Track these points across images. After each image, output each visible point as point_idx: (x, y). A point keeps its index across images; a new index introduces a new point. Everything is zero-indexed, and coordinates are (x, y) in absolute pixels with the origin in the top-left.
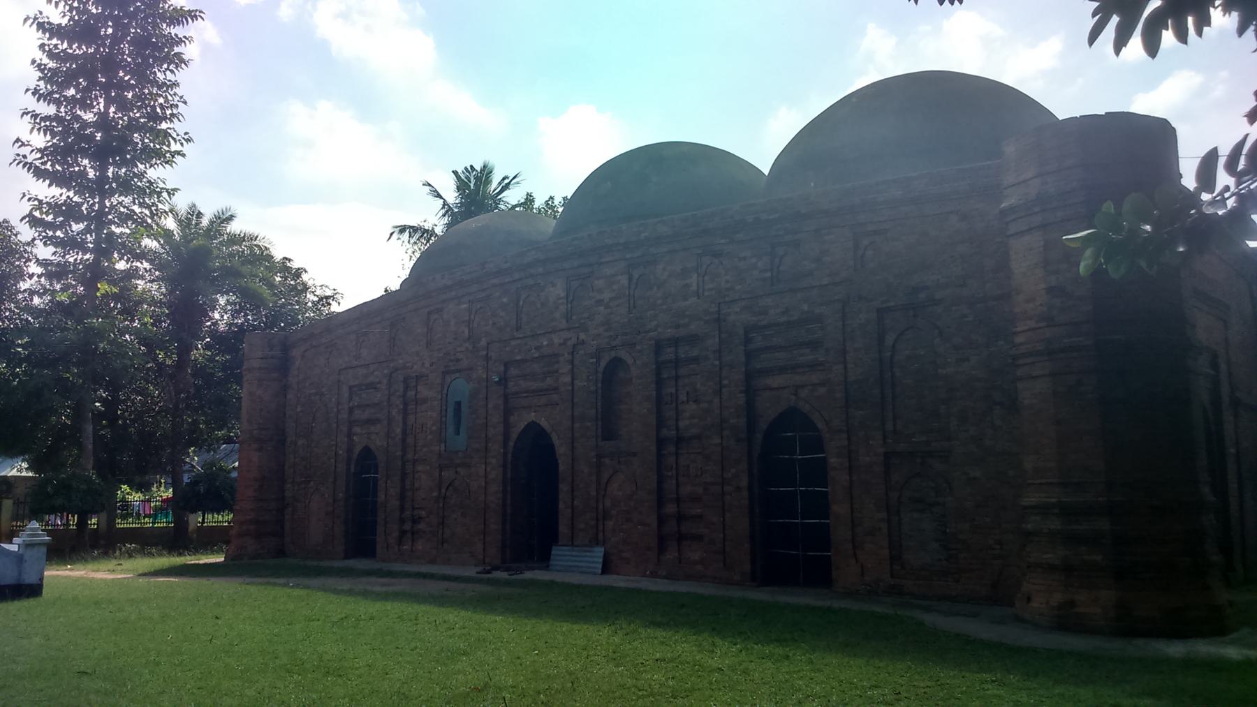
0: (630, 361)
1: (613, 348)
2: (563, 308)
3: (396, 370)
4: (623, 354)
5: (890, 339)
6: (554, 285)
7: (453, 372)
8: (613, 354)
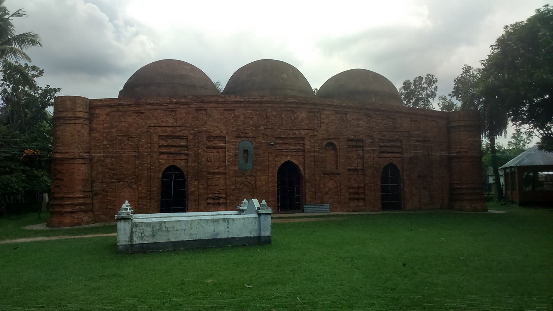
0: (336, 143)
1: (329, 139)
4: (333, 141)
6: (301, 113)
7: (242, 137)
8: (329, 141)
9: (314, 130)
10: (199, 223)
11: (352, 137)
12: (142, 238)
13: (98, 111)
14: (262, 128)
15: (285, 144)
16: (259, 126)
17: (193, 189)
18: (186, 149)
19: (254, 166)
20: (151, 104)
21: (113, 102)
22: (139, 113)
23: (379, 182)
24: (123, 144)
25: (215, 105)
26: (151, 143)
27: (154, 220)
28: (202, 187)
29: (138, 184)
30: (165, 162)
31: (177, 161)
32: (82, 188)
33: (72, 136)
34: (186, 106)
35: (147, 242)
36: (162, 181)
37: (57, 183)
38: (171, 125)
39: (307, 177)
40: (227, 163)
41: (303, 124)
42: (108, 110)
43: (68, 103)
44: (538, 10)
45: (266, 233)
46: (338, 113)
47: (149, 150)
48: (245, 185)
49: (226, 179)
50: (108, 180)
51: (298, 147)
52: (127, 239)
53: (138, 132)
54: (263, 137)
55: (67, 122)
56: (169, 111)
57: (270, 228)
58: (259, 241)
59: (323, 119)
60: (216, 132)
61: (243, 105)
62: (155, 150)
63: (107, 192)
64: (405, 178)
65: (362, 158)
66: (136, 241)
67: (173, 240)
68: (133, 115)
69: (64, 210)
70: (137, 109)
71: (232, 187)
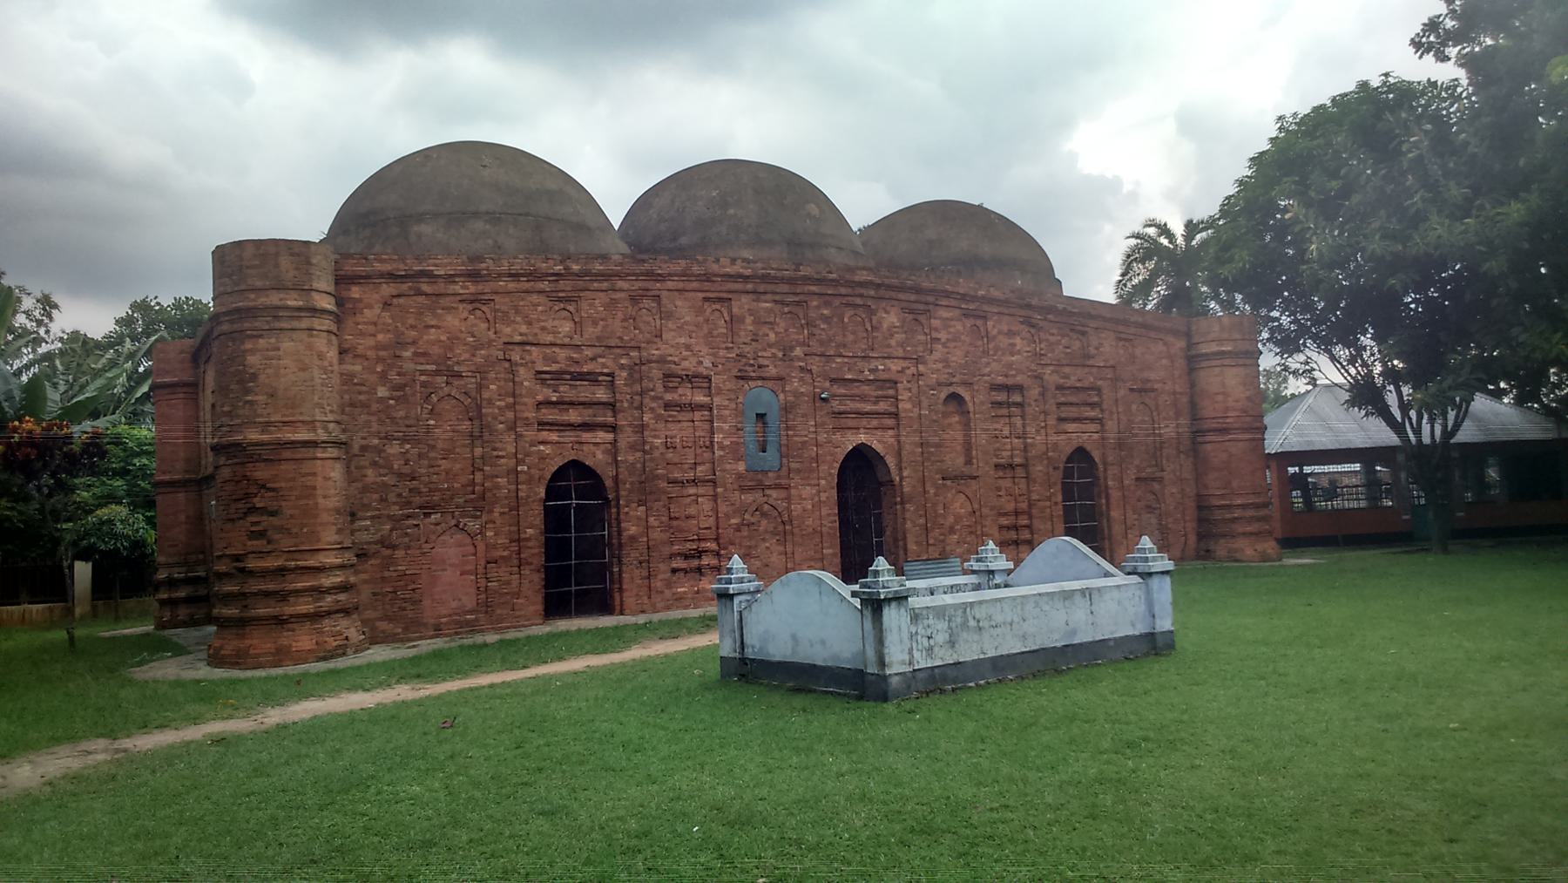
0: (967, 398)
1: (951, 384)
2: (899, 337)
3: (650, 362)
4: (961, 391)
5: (1134, 407)
6: (887, 312)
7: (752, 379)
8: (952, 389)
9: (918, 361)
10: (1037, 603)
11: (1000, 380)
12: (930, 649)
13: (355, 292)
14: (798, 351)
15: (852, 397)
16: (792, 348)
17: (633, 530)
18: (610, 413)
20: (510, 275)
21: (402, 266)
22: (475, 301)
23: (1060, 498)
24: (434, 398)
25: (681, 285)
26: (514, 395)
27: (949, 599)
28: (656, 524)
29: (484, 518)
30: (552, 451)
31: (585, 448)
32: (336, 538)
33: (303, 370)
34: (605, 285)
35: (939, 663)
36: (548, 511)
37: (253, 524)
38: (567, 341)
39: (906, 490)
40: (718, 453)
41: (893, 342)
42: (387, 289)
43: (285, 262)
44: (1364, 86)
45: (1165, 624)
46: (966, 314)
47: (510, 415)
48: (764, 515)
49: (715, 497)
50: (396, 511)
51: (882, 406)
52: (907, 657)
53: (479, 360)
54: (801, 379)
55: (284, 325)
56: (560, 300)
57: (1169, 608)
58: (1153, 645)
59: (936, 330)
60: (685, 364)
61: (750, 287)
62: (526, 414)
63: (394, 547)
64: (1110, 483)
65: (1023, 436)
66: (922, 662)
67: (991, 653)
68: (461, 306)
69: (289, 610)
70: (472, 288)
71: (733, 521)
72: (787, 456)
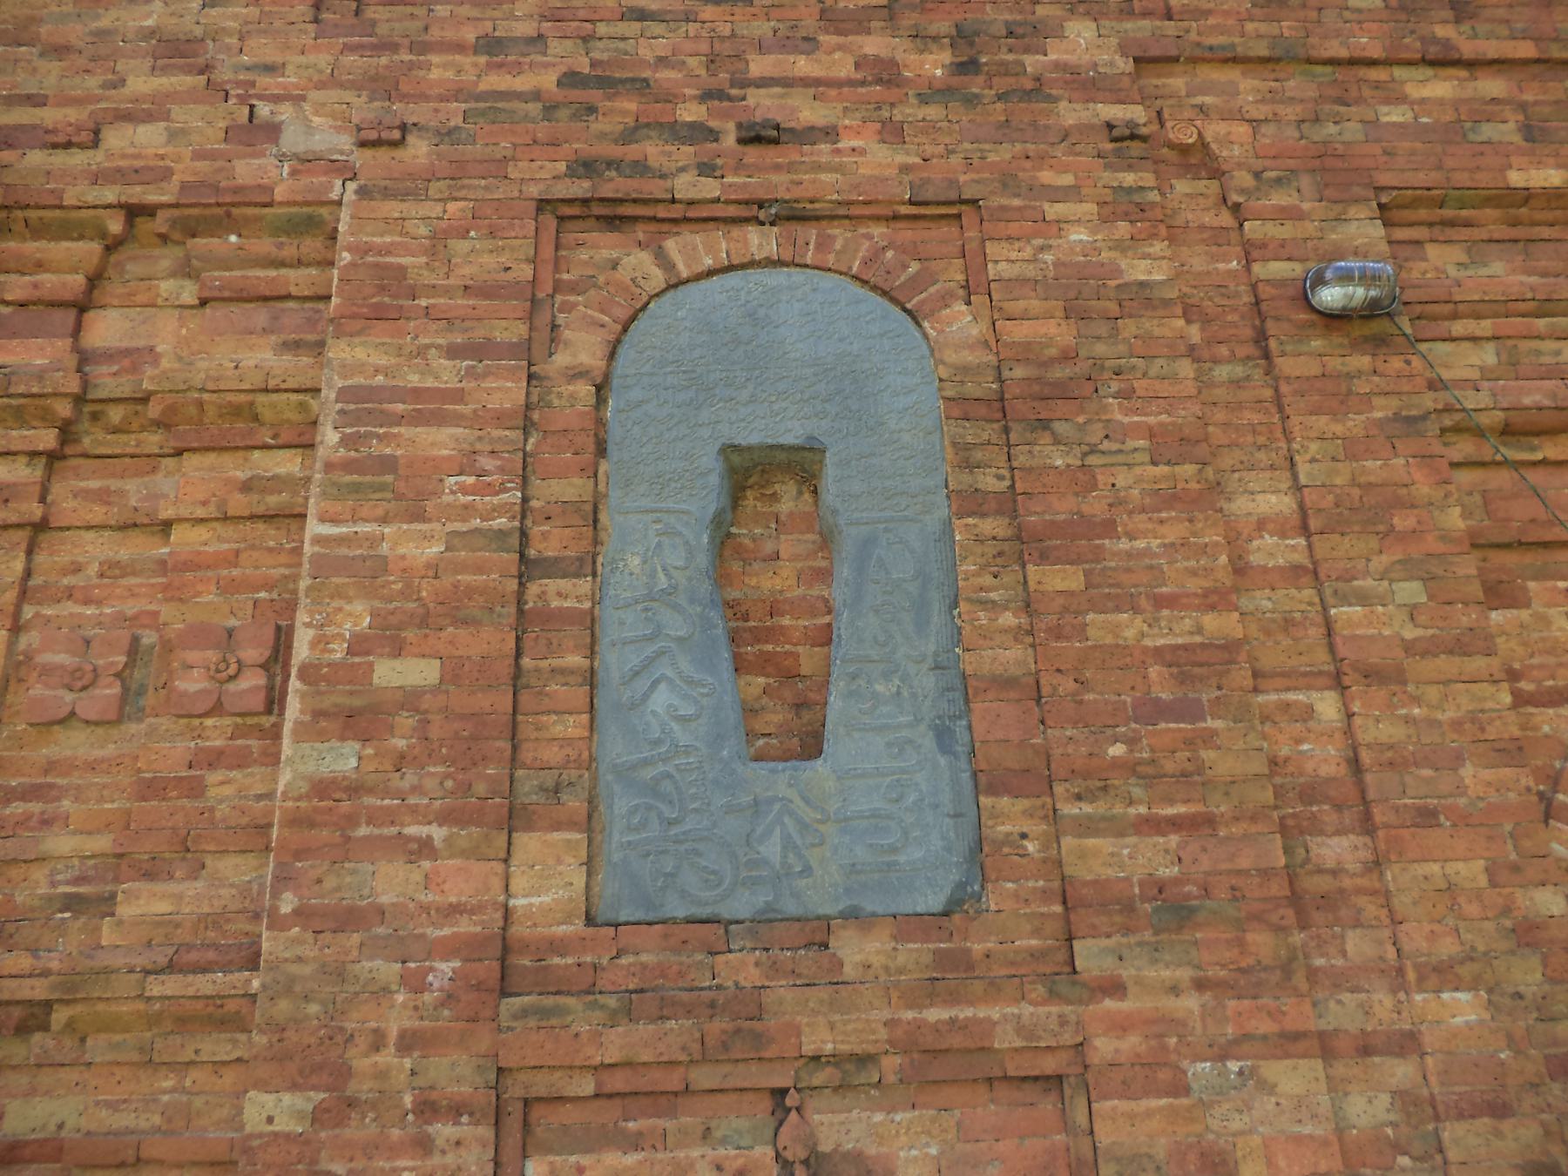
7: (693, 216)
19: (1011, 816)
54: (1123, 207)
72: (1035, 778)
